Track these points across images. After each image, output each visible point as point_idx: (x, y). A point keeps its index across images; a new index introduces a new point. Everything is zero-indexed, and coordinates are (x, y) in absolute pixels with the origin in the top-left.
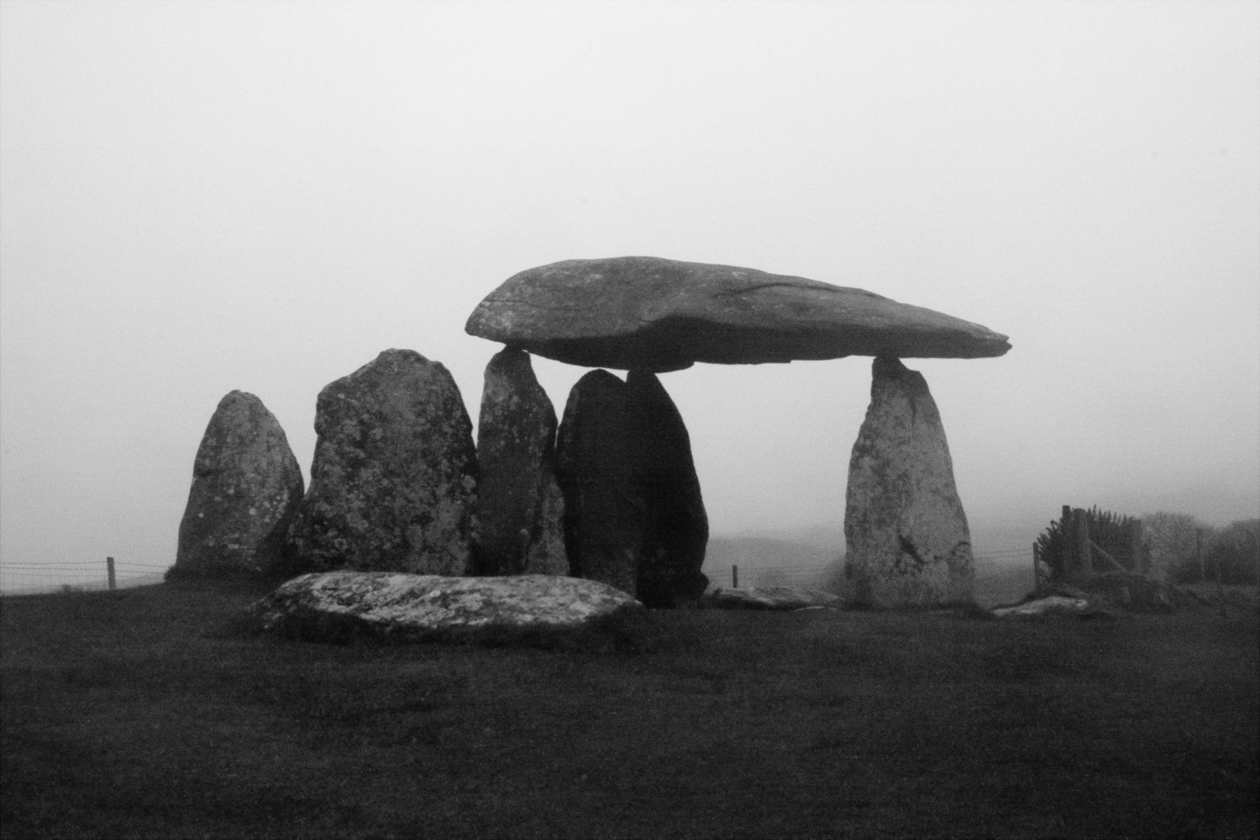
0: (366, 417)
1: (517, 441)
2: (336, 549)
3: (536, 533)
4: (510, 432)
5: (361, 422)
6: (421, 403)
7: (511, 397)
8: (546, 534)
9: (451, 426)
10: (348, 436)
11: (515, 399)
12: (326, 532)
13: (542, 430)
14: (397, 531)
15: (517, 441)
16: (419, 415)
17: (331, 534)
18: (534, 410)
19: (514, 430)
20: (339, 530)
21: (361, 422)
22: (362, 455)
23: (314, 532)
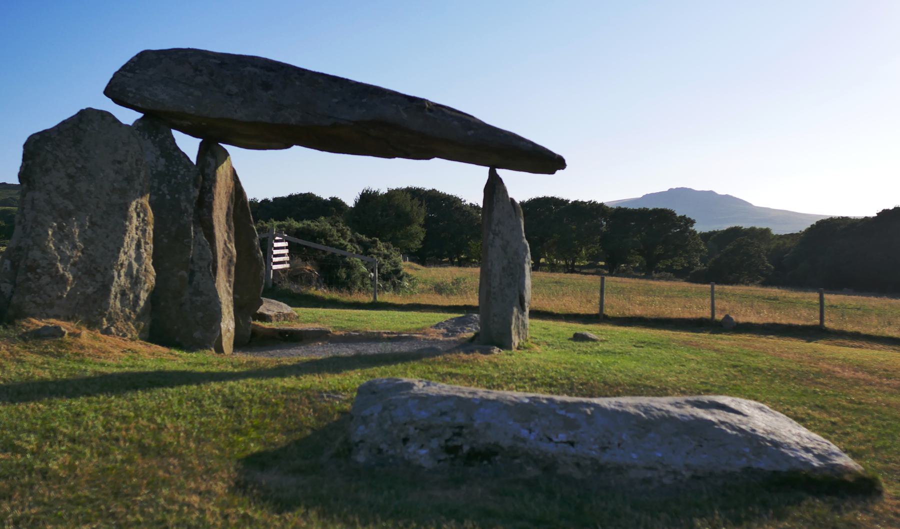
0: (72, 170)
1: (168, 197)
2: (50, 296)
3: (192, 274)
4: (159, 190)
5: (70, 176)
6: (119, 162)
7: (157, 158)
8: (198, 275)
9: (140, 185)
10: (58, 188)
11: (162, 161)
12: (39, 279)
13: (191, 190)
14: (99, 277)
15: (168, 197)
16: (117, 172)
17: (45, 279)
18: (182, 172)
19: (165, 189)
20: (51, 277)
21: (70, 176)
22: (72, 207)
23: (28, 279)
